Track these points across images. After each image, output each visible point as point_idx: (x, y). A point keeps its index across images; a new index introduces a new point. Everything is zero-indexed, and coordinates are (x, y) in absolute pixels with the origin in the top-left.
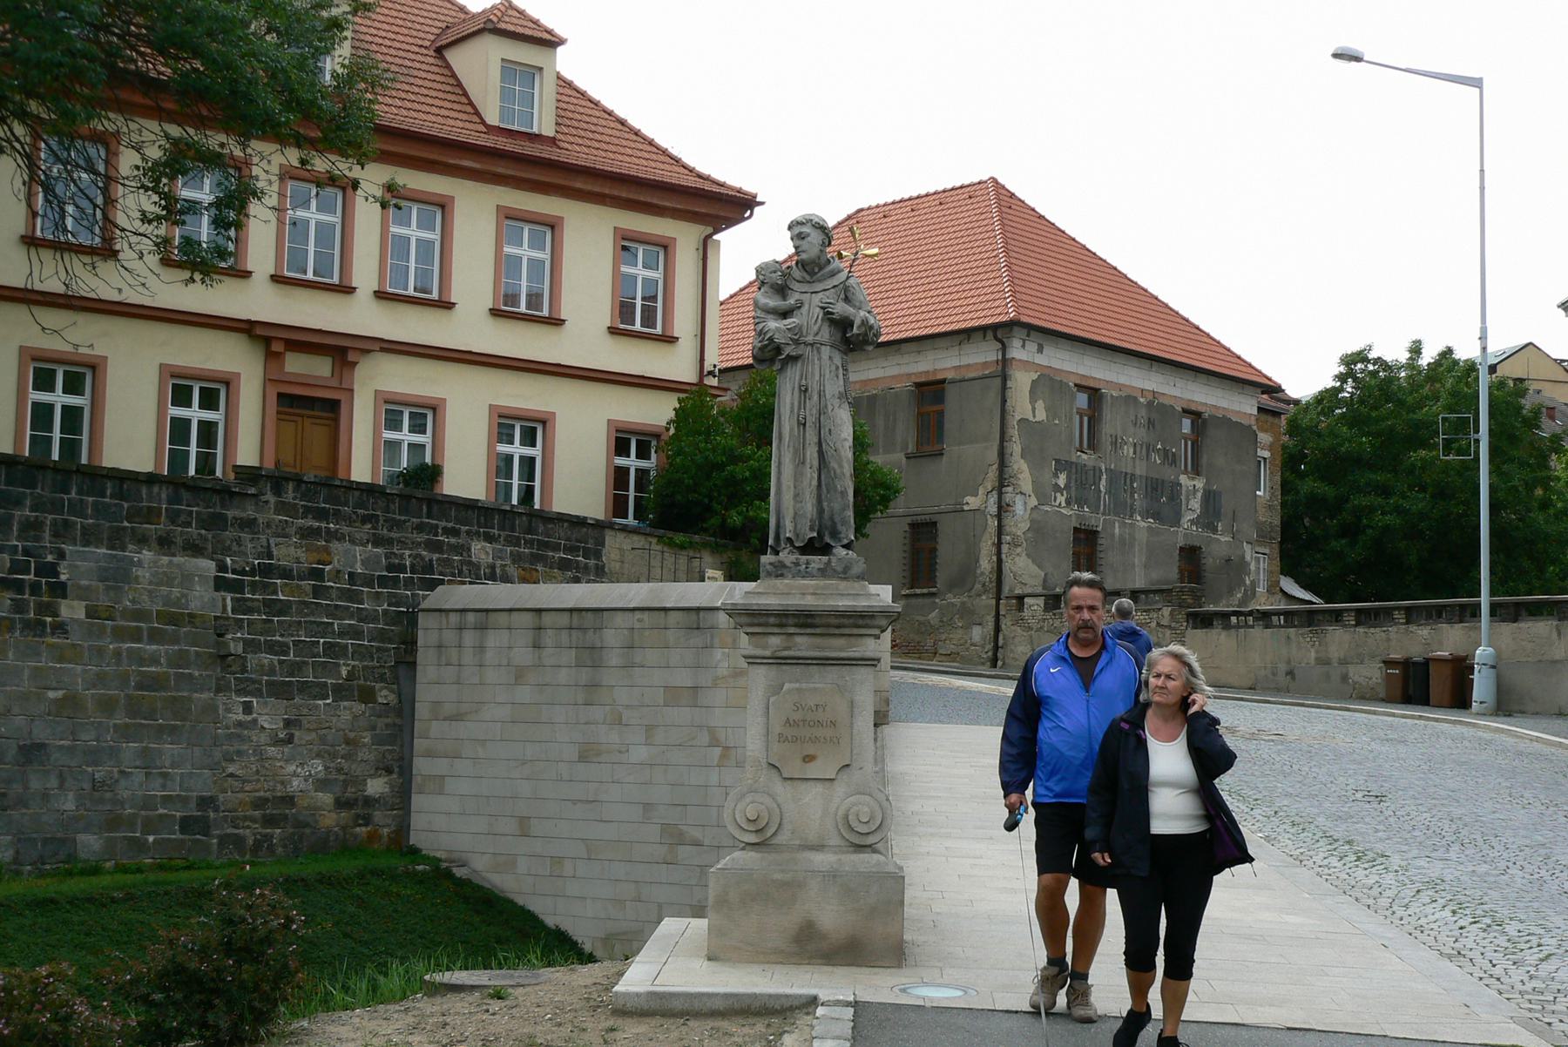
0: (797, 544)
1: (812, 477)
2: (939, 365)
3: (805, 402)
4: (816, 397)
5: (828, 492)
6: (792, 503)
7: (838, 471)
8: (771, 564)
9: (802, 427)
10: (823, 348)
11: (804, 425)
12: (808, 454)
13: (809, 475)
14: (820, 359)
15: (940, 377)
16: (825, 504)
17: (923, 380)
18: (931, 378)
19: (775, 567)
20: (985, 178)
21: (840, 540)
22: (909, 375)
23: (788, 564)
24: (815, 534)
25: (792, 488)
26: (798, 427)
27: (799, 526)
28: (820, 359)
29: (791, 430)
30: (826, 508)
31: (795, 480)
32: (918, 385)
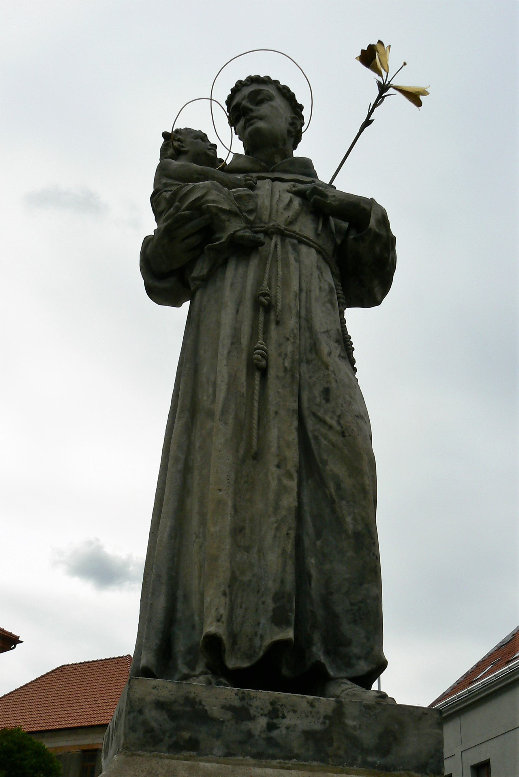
0: (231, 663)
1: (283, 489)
2: (95, 742)
3: (266, 331)
4: (292, 323)
5: (318, 535)
6: (227, 545)
7: (348, 483)
8: (160, 705)
9: (257, 375)
10: (304, 249)
11: (264, 372)
12: (273, 434)
13: (274, 484)
14: (298, 260)
15: (95, 747)
16: (312, 561)
17: (86, 748)
18: (90, 748)
19: (174, 716)
20: (125, 655)
21: (349, 665)
22: (79, 746)
23: (216, 712)
24: (290, 634)
25: (229, 510)
26: (250, 374)
27: (239, 612)
28: (298, 260)
29: (233, 379)
30: (314, 572)
31: (237, 493)
32: (84, 751)
